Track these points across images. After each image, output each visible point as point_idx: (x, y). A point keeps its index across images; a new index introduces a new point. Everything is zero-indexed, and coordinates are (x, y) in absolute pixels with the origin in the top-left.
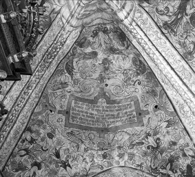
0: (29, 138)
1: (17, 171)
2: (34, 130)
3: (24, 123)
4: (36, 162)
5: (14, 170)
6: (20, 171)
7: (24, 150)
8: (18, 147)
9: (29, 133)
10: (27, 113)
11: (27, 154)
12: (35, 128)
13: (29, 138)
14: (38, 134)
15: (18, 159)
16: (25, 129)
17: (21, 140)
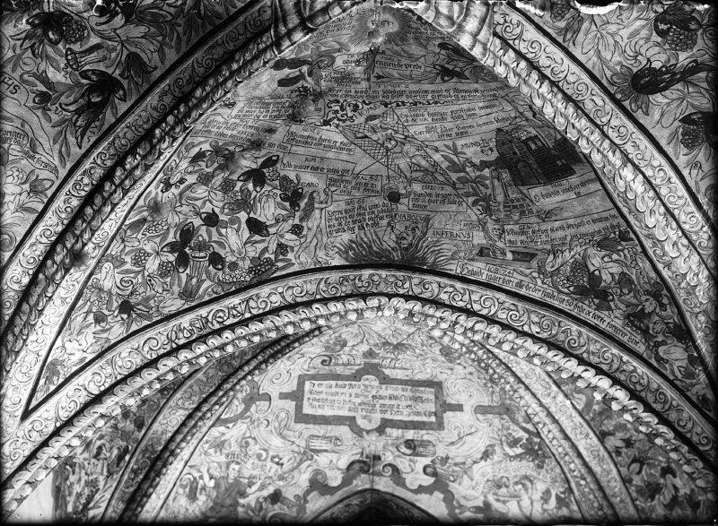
0: (620, 444)
1: (653, 499)
2: (611, 428)
3: (587, 435)
4: (663, 468)
5: (649, 500)
6: (657, 497)
7: (633, 461)
8: (621, 466)
9: (612, 438)
10: (572, 421)
11: (642, 464)
12: (609, 425)
13: (620, 444)
14: (622, 427)
15: (637, 480)
16: (599, 440)
17: (614, 455)
